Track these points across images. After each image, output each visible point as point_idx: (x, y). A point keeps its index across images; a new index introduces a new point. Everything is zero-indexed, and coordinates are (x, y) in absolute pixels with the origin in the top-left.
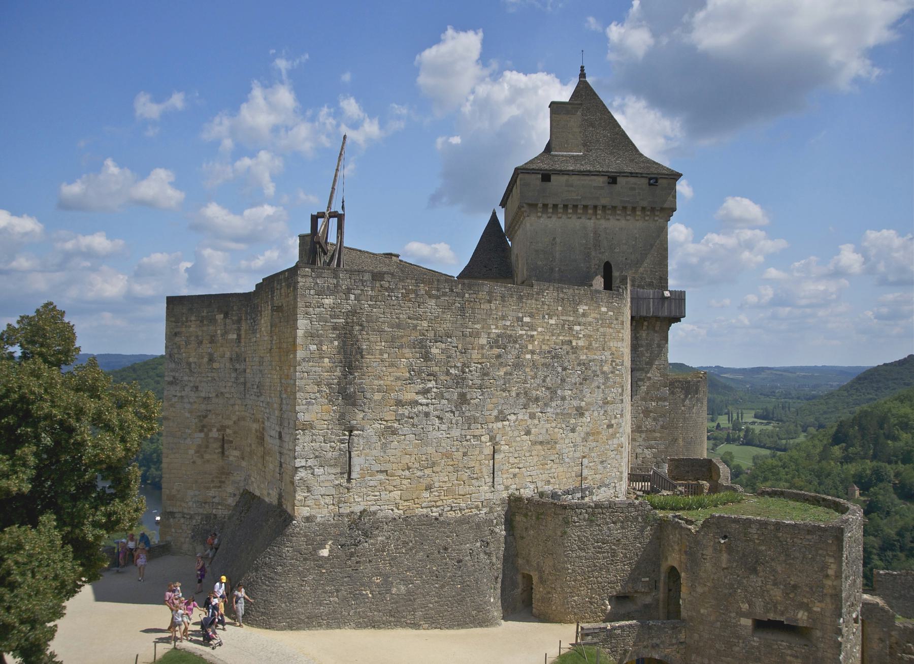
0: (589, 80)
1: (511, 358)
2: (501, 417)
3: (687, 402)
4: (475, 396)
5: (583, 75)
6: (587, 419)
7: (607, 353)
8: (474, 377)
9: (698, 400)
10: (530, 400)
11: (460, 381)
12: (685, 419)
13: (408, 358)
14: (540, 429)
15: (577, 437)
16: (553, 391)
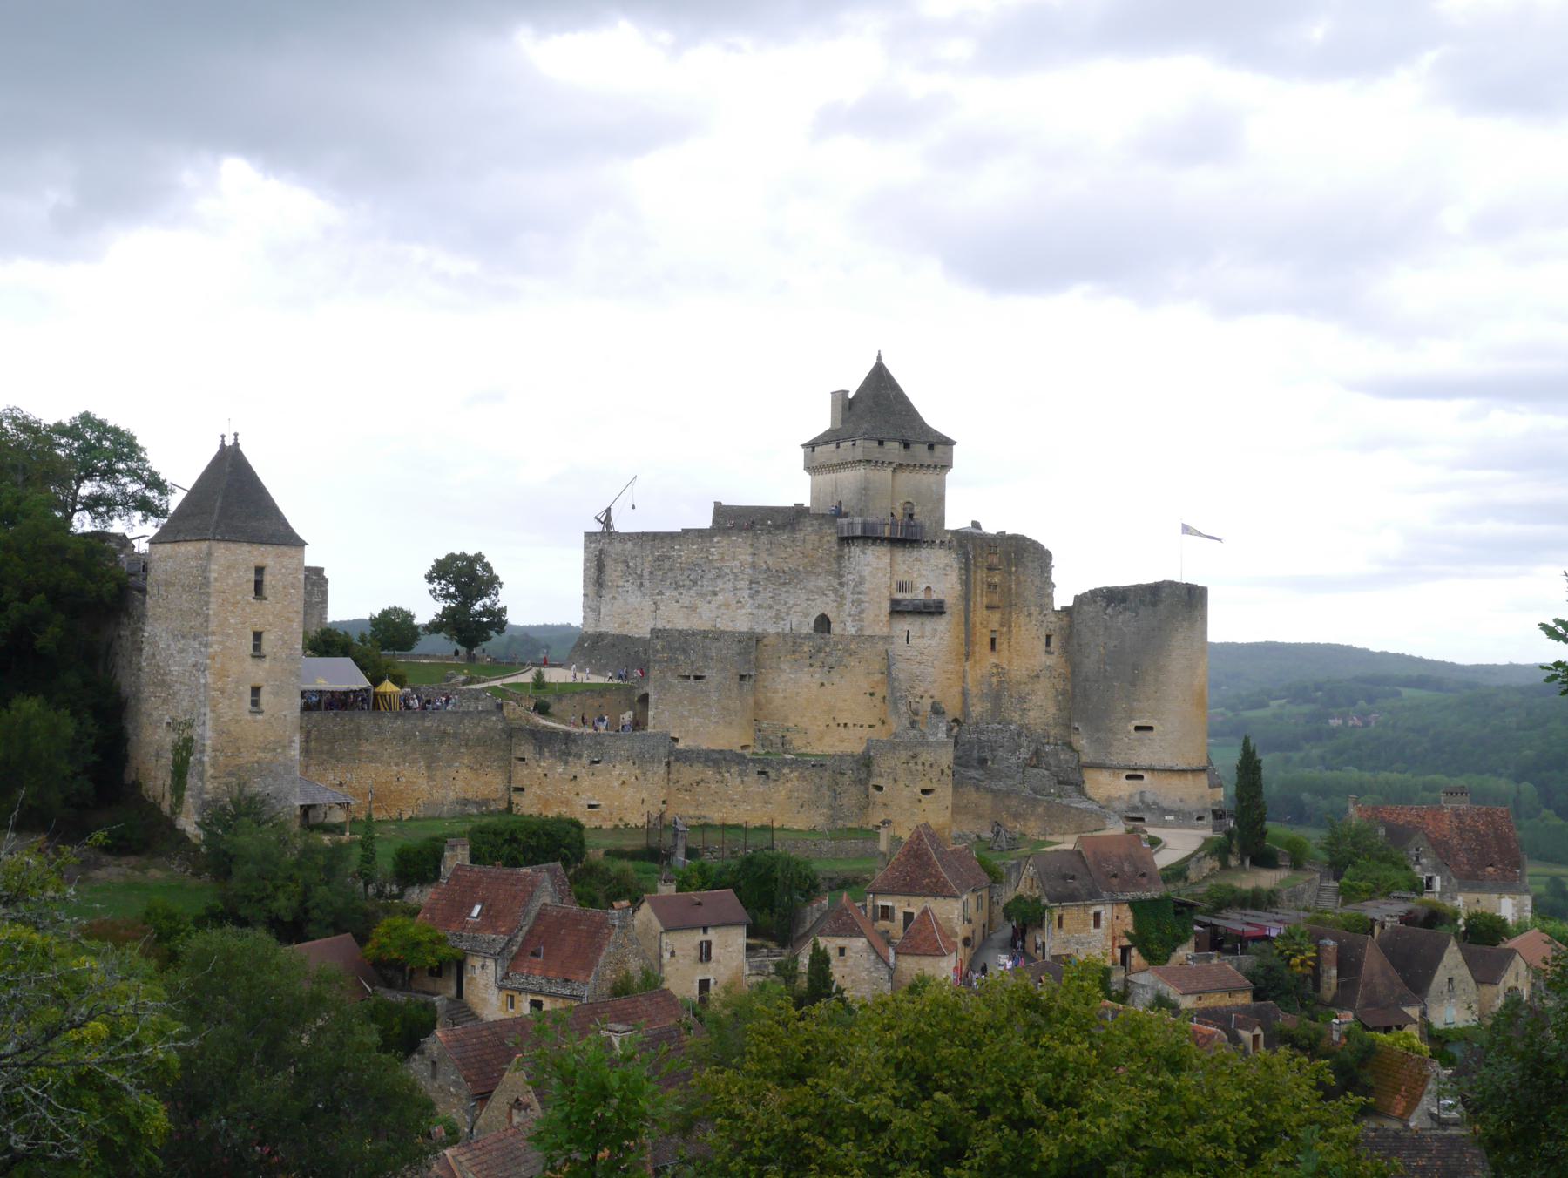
0: (885, 361)
1: (666, 566)
2: (660, 593)
3: (1109, 611)
4: (647, 584)
5: (879, 358)
6: (720, 596)
7: (737, 563)
8: (646, 575)
9: (1125, 609)
10: (678, 586)
11: (641, 576)
12: (1106, 628)
13: (621, 567)
14: (686, 600)
15: (714, 605)
16: (695, 583)
